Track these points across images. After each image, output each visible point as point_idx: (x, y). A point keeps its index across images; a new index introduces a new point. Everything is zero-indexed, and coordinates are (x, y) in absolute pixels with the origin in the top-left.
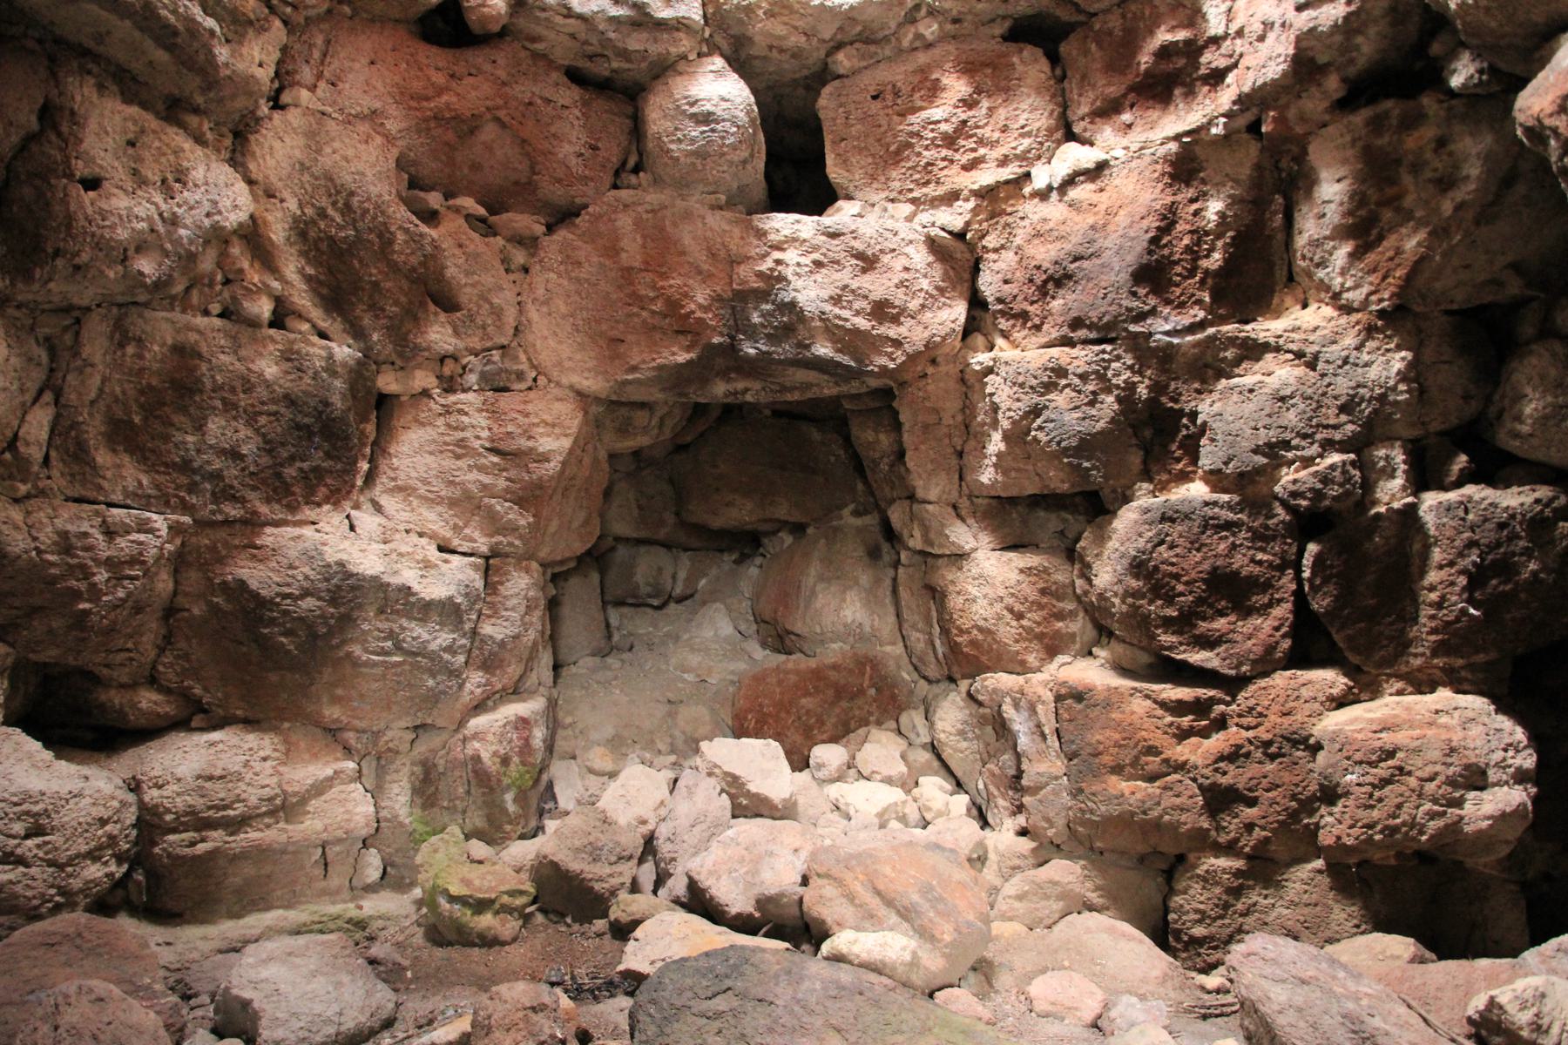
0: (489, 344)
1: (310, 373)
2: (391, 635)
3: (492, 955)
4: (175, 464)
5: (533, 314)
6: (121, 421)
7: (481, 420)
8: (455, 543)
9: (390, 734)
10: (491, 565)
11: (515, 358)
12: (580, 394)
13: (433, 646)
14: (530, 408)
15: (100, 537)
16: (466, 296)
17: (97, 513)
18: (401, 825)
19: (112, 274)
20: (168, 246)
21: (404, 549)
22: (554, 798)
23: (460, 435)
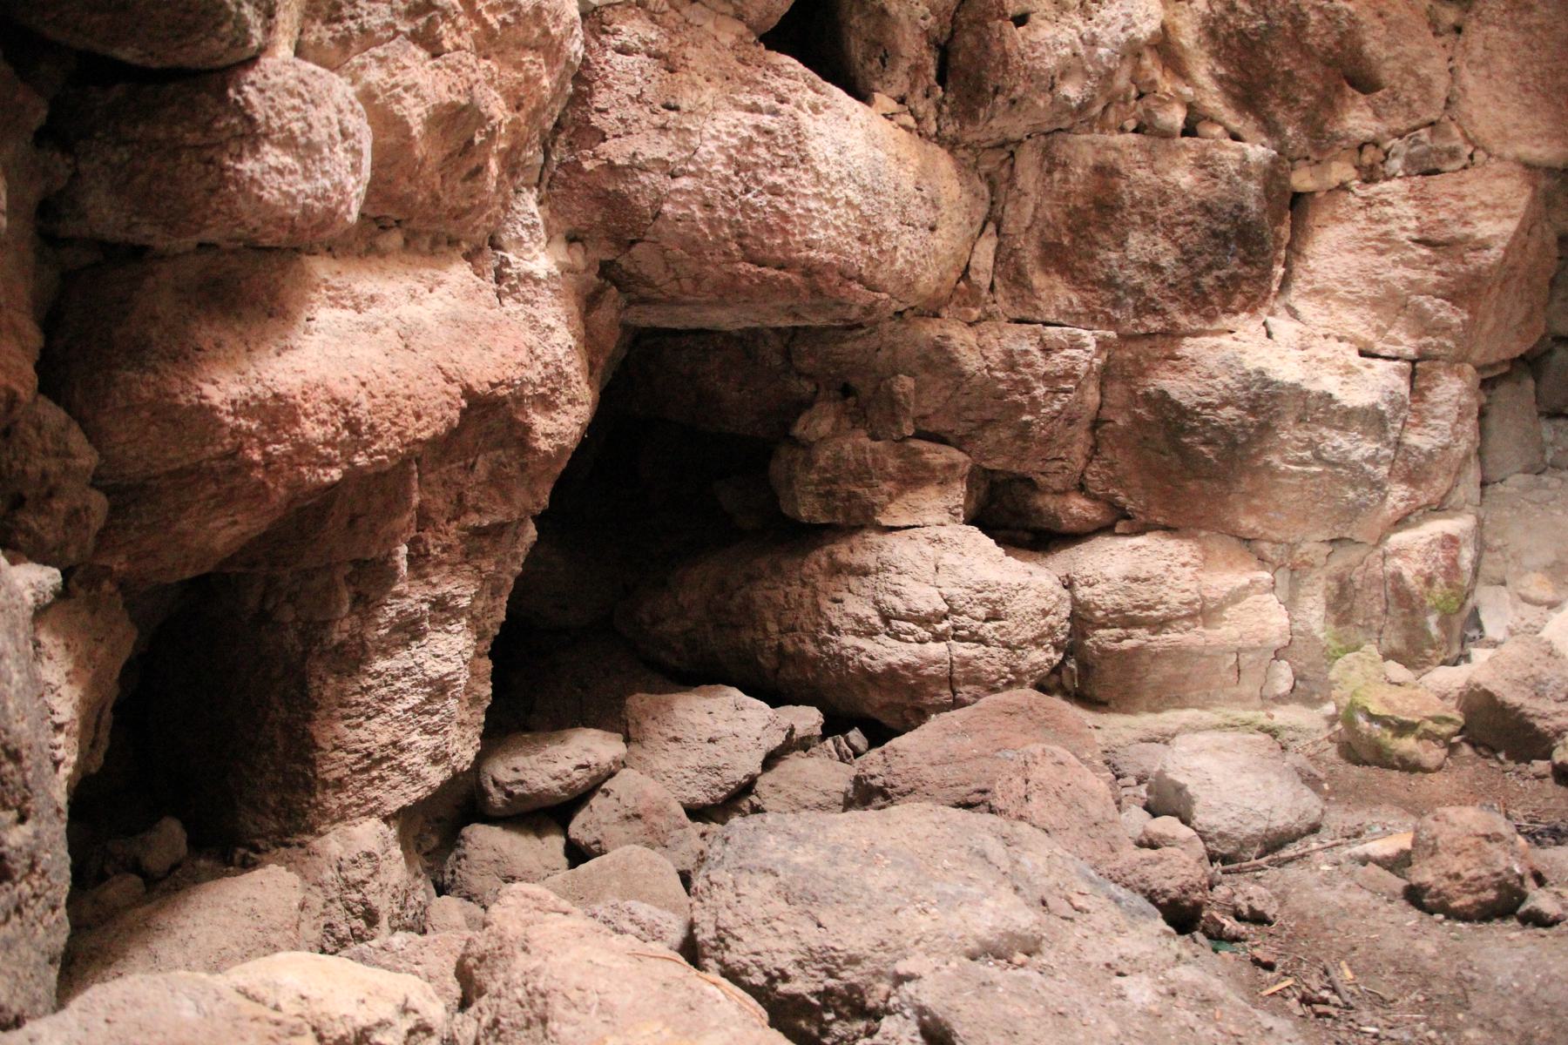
0: (1415, 123)
1: (1224, 177)
2: (1310, 444)
3: (1414, 779)
4: (1100, 280)
5: (1469, 80)
6: (1053, 244)
7: (1408, 209)
8: (1378, 346)
9: (1305, 547)
10: (1418, 370)
11: (1447, 135)
12: (1529, 167)
13: (1355, 456)
14: (1465, 189)
15: (1039, 354)
16: (1388, 72)
17: (1036, 332)
18: (1315, 639)
19: (1041, 103)
20: (1090, 68)
21: (1323, 355)
22: (1479, 626)
23: (1383, 228)
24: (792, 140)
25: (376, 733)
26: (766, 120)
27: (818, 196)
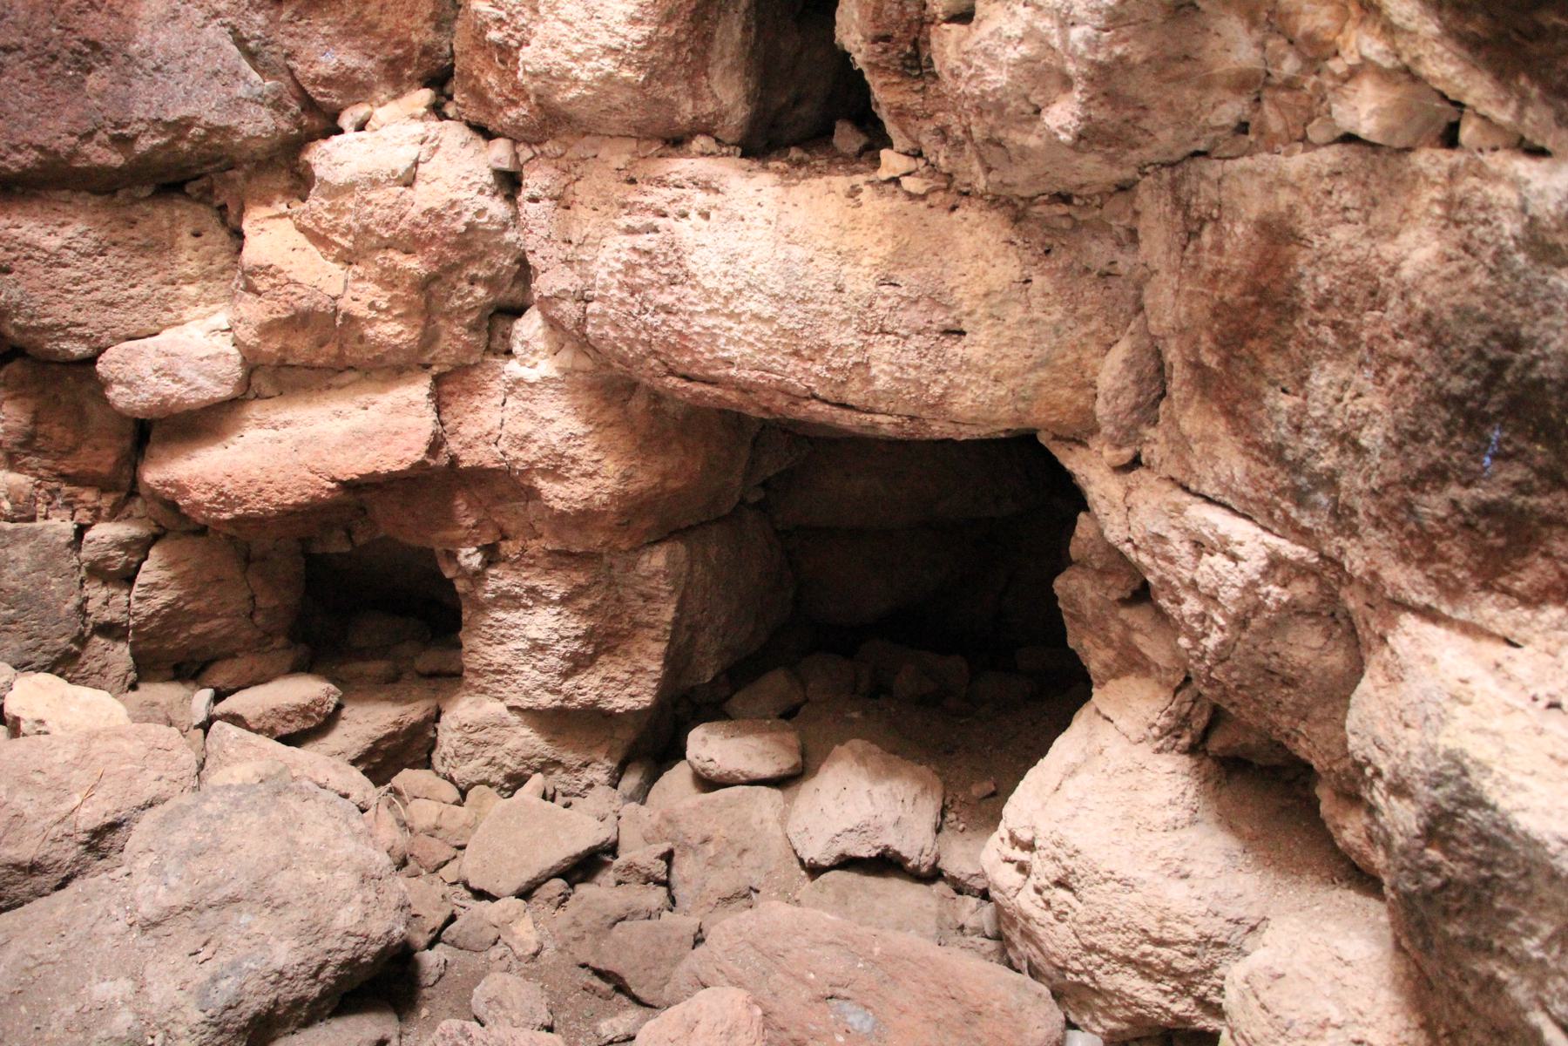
1: (1487, 254)
24: (672, 257)
25: (499, 655)
26: (642, 241)
27: (710, 312)
